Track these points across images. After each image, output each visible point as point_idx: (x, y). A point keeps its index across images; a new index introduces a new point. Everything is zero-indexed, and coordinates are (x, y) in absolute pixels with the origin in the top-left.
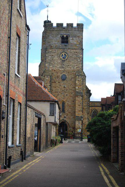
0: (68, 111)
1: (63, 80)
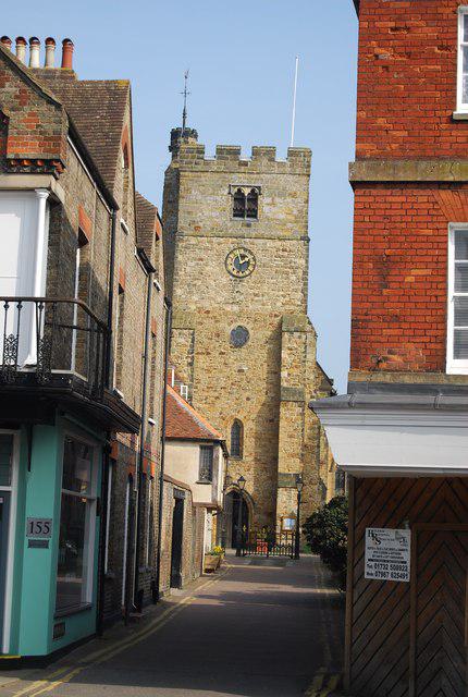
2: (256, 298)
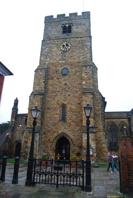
0: (70, 119)
1: (65, 75)
2: (72, 57)
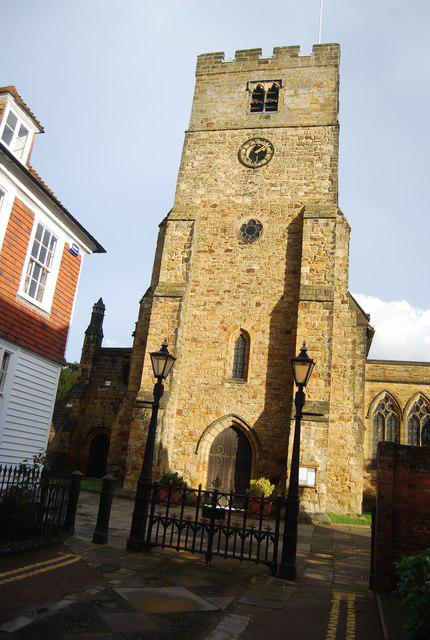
2: (273, 188)
